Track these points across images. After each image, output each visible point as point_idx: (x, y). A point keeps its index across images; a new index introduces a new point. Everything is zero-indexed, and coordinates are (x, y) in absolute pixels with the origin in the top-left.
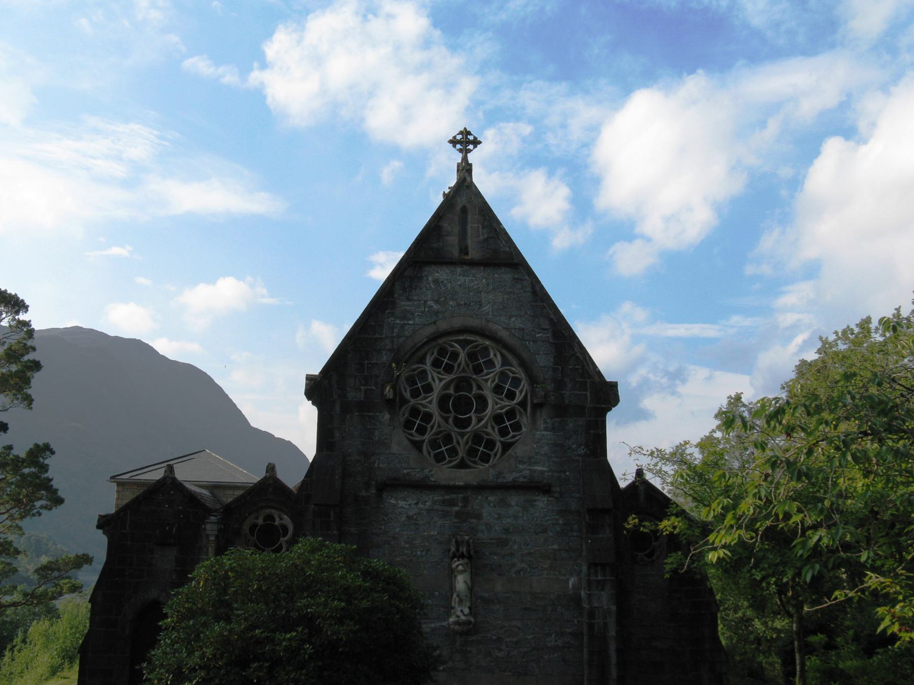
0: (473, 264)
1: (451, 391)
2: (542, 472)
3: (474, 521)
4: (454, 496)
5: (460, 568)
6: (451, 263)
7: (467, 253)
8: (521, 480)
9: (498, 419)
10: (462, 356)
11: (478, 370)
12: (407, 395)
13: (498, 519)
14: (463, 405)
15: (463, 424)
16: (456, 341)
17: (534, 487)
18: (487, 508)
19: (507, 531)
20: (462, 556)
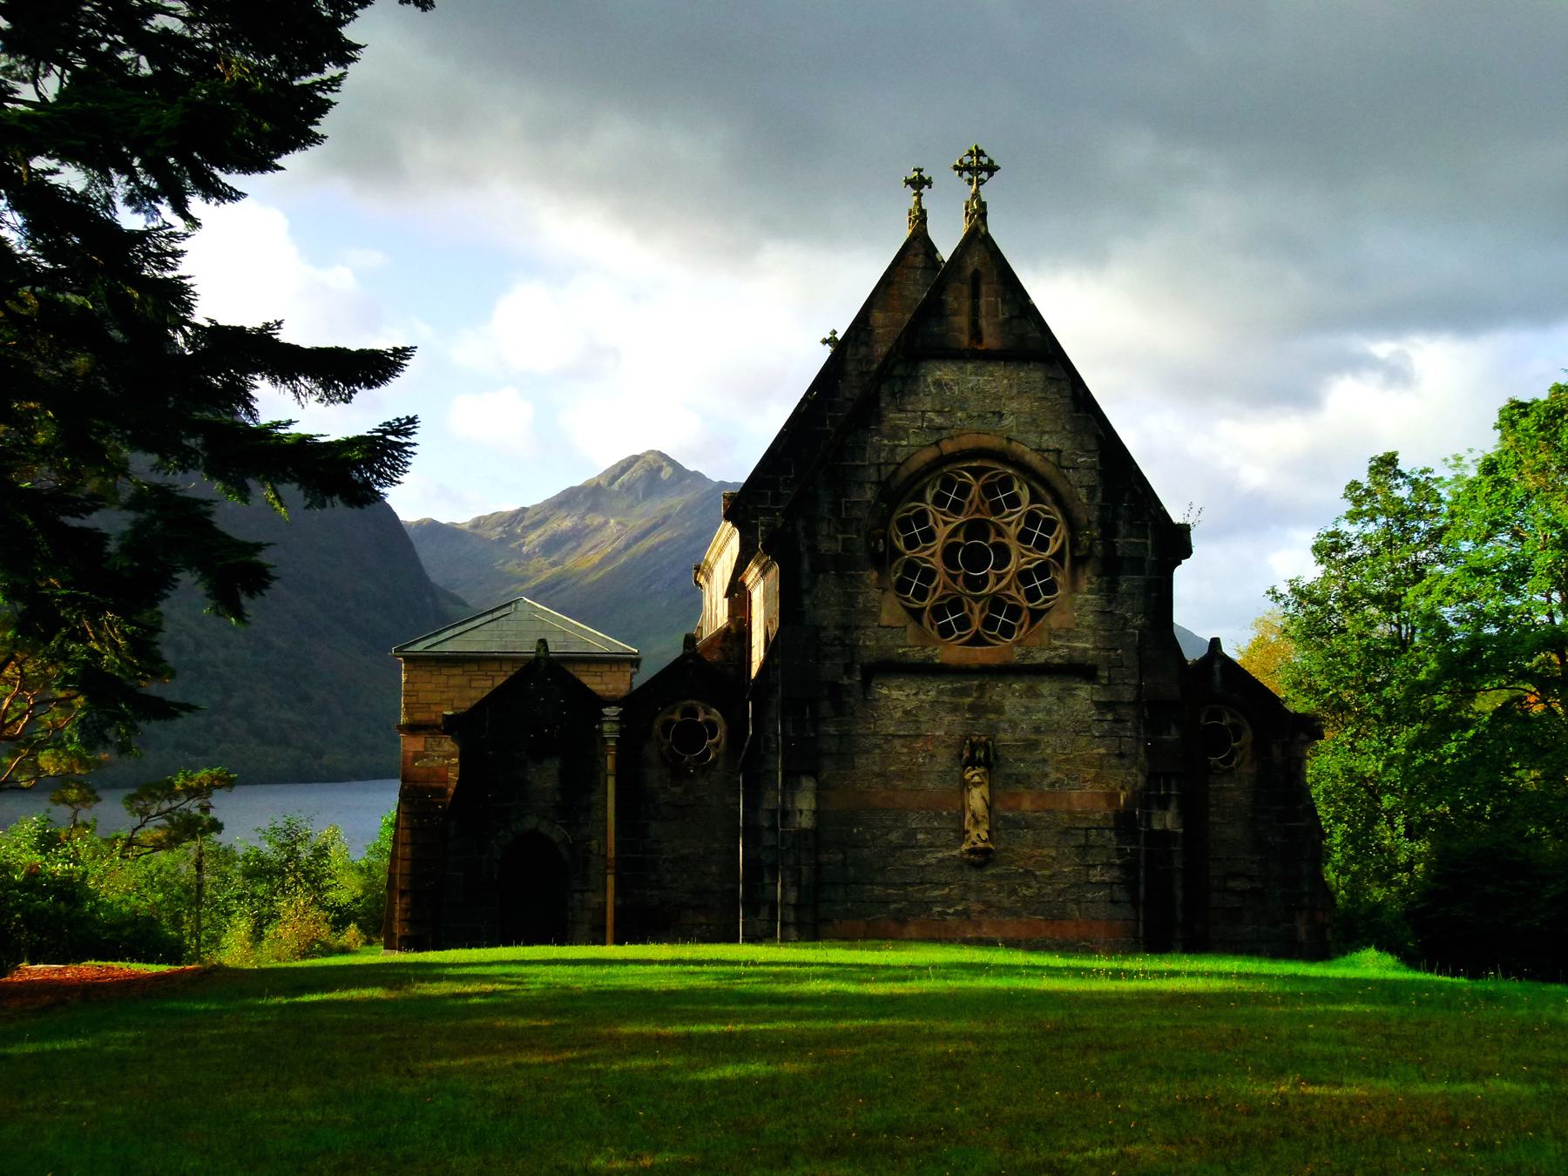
0: (990, 357)
1: (960, 539)
2: (1085, 650)
3: (992, 716)
4: (966, 683)
5: (976, 779)
7: (980, 341)
8: (1057, 660)
9: (1024, 577)
10: (975, 490)
11: (996, 509)
12: (901, 545)
13: (1026, 713)
14: (976, 558)
15: (977, 584)
16: (968, 469)
17: (1074, 670)
18: (1011, 698)
19: (1037, 730)
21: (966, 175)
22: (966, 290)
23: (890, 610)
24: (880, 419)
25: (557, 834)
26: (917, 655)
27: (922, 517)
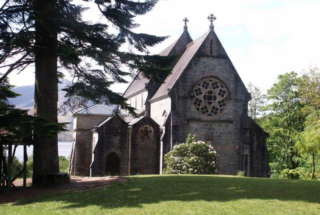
0: (214, 57)
6: (208, 56)
10: (210, 84)
11: (214, 88)
12: (195, 95)
14: (210, 98)
17: (229, 121)
18: (216, 127)
19: (221, 133)
20: (210, 140)
21: (210, 19)
22: (210, 43)
23: (193, 108)
24: (192, 68)
25: (118, 153)
26: (198, 117)
27: (199, 89)
